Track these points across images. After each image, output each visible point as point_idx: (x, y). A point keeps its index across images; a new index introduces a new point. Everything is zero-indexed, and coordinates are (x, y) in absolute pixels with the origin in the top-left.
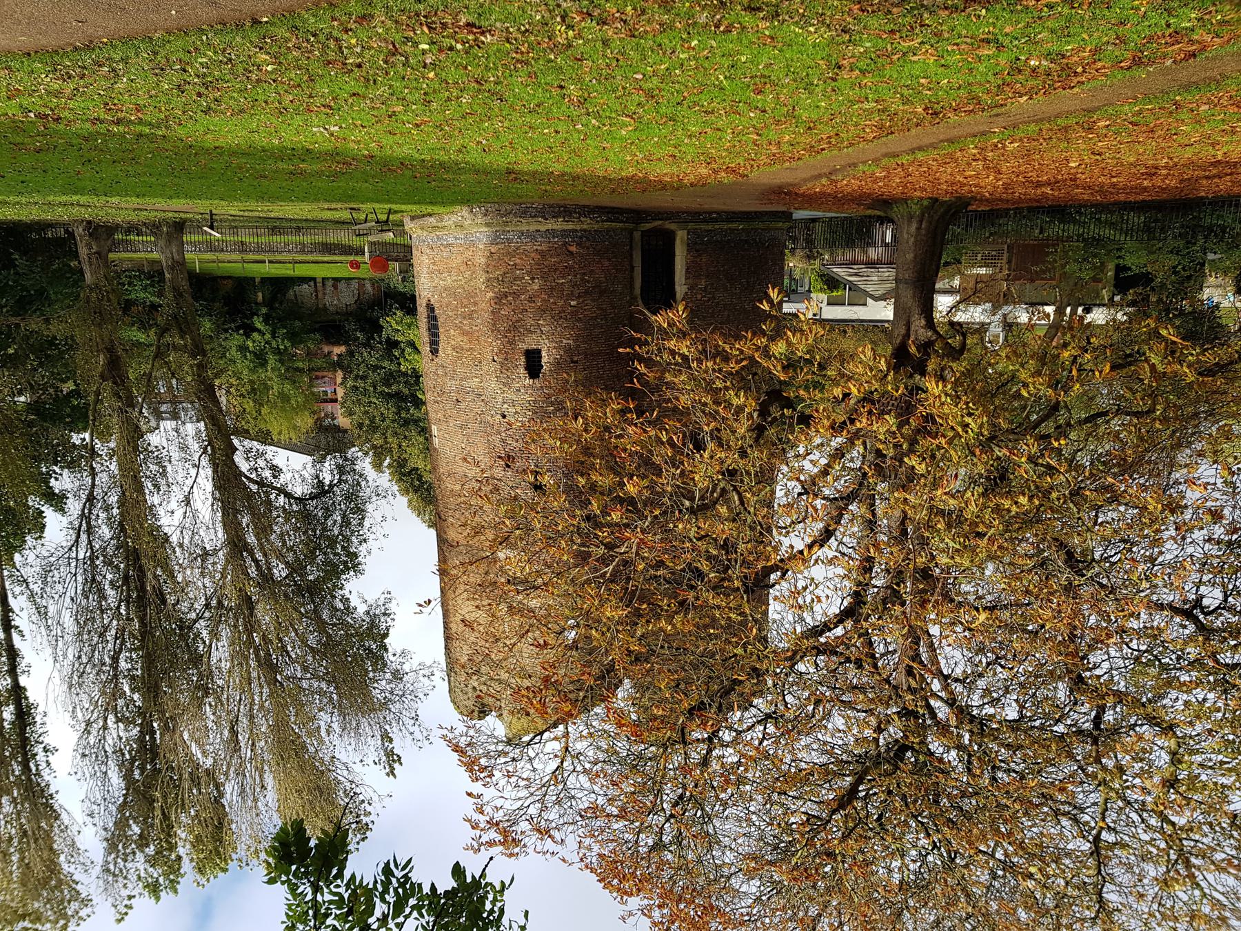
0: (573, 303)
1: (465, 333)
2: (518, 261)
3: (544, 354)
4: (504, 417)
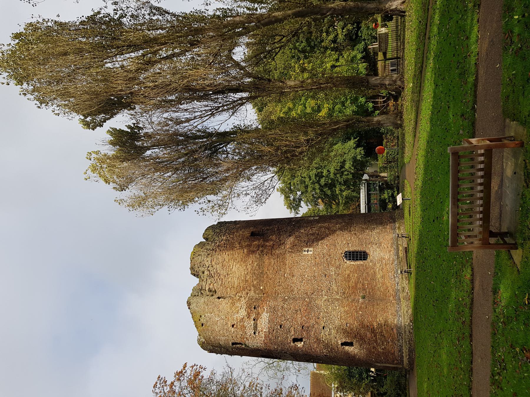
1: (356, 284)
4: (323, 328)
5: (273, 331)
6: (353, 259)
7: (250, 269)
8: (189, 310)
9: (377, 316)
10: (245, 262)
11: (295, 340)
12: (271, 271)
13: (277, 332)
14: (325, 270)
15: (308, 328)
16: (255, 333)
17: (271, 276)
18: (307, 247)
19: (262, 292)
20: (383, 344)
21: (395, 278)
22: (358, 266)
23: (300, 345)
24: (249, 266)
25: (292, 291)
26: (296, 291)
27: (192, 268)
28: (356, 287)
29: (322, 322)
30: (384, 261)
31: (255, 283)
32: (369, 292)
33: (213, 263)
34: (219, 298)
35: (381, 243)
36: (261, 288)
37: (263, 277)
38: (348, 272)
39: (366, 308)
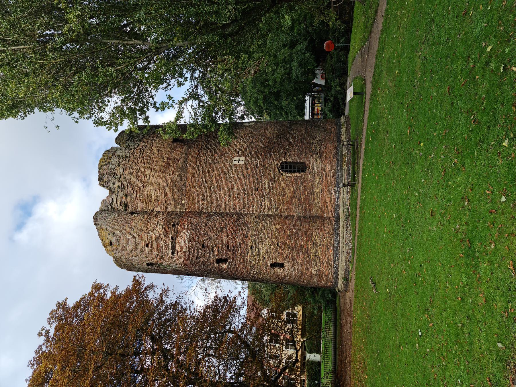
0: (305, 281)
1: (292, 199)
2: (325, 265)
4: (251, 248)
5: (194, 251)
6: (289, 171)
7: (169, 181)
8: (95, 227)
9: (312, 234)
10: (164, 172)
11: (219, 261)
12: (194, 183)
13: (199, 252)
15: (234, 247)
16: (173, 253)
17: (194, 189)
19: (184, 206)
20: (317, 265)
22: (296, 178)
23: (224, 266)
24: (169, 177)
25: (219, 206)
26: (222, 207)
27: (100, 179)
28: (292, 201)
29: (250, 241)
30: (324, 173)
31: (176, 196)
32: (306, 208)
33: (126, 172)
34: (132, 213)
36: (183, 202)
37: (186, 190)
38: (283, 185)
39: (301, 225)
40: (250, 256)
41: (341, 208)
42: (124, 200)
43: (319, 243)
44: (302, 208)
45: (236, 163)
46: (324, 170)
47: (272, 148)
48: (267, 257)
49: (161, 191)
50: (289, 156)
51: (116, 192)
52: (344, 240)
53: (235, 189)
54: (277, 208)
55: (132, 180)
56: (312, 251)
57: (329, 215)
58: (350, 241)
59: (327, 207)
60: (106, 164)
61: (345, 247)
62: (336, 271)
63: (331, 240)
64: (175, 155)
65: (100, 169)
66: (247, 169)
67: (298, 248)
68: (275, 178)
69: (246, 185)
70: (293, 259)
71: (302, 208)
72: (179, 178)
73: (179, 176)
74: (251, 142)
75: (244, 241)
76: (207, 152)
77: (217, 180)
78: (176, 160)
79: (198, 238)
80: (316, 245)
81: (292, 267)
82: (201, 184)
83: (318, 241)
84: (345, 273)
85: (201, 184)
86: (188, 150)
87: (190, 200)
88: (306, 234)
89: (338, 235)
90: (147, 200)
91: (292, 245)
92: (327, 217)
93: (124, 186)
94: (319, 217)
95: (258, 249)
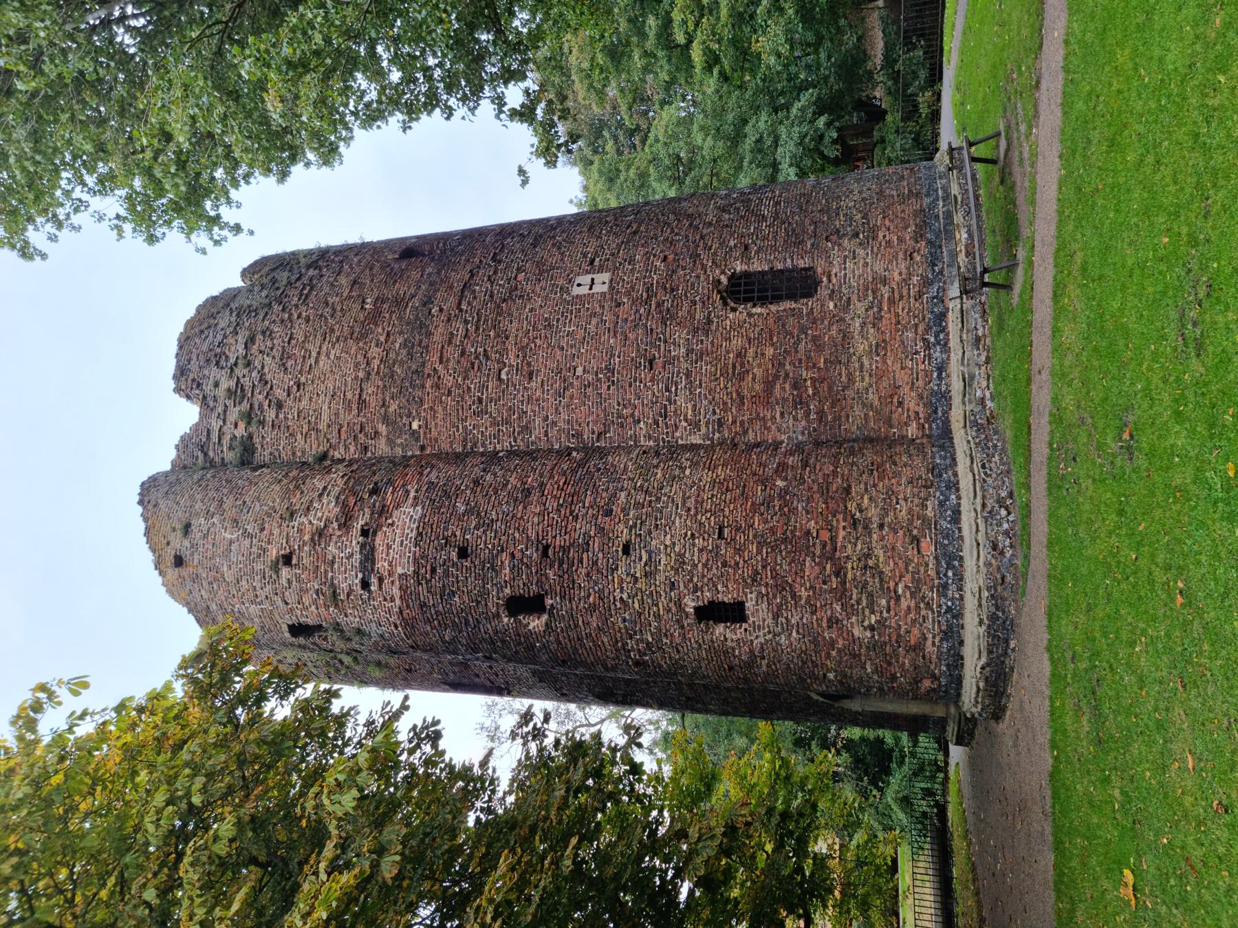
0: (831, 676)
1: (769, 385)
2: (904, 604)
3: (740, 633)
4: (626, 550)
5: (433, 570)
7: (377, 362)
9: (847, 490)
10: (363, 336)
12: (451, 364)
13: (447, 573)
14: (653, 345)
16: (365, 585)
17: (448, 381)
18: (588, 272)
19: (417, 439)
20: (871, 606)
21: (927, 346)
23: (536, 623)
24: (375, 352)
25: (526, 429)
27: (181, 373)
29: (621, 526)
30: (885, 291)
31: (391, 409)
32: (821, 414)
35: (873, 232)
36: (415, 426)
37: (423, 386)
38: (737, 343)
39: (805, 465)
40: (621, 581)
41: (956, 400)
42: (241, 431)
43: (875, 519)
44: (807, 414)
45: (584, 290)
46: (884, 281)
47: (702, 237)
48: (680, 580)
49: (349, 395)
50: (757, 252)
51: (220, 409)
52: (979, 500)
53: (579, 371)
54: (720, 423)
55: (266, 370)
56: (851, 551)
57: (912, 431)
58: (1001, 502)
59: (900, 404)
60: (202, 332)
61: (982, 527)
62: (950, 627)
63: (924, 507)
64: (401, 288)
65: (181, 347)
66: (618, 305)
67: (797, 544)
68: (710, 322)
69: (612, 356)
70: (781, 586)
71: (807, 414)
72: (404, 352)
73: (404, 345)
74: (635, 233)
75: (601, 530)
76: (495, 273)
77: (522, 349)
78: (399, 302)
79: (446, 529)
80: (866, 527)
81: (776, 617)
82: (471, 365)
83: (873, 513)
84: (991, 633)
85: (471, 365)
86: (439, 273)
87: (434, 417)
88: (825, 490)
89: (954, 486)
90: (306, 427)
91: (773, 531)
92: (903, 437)
93: (243, 390)
94: (871, 440)
95: (650, 553)
